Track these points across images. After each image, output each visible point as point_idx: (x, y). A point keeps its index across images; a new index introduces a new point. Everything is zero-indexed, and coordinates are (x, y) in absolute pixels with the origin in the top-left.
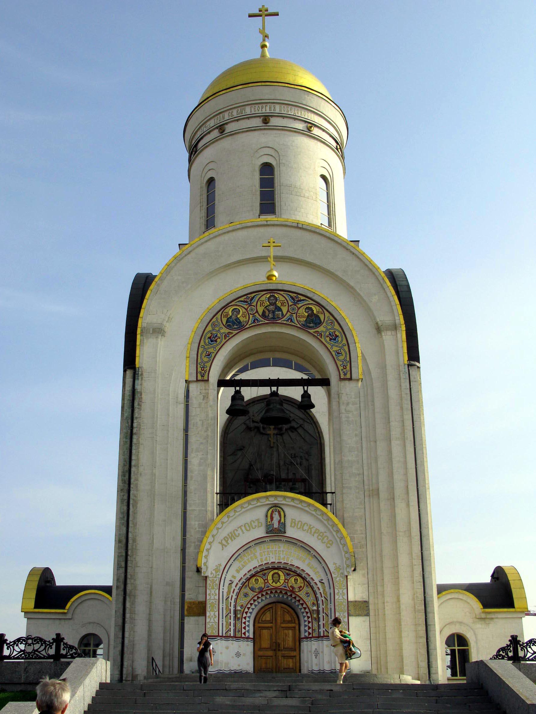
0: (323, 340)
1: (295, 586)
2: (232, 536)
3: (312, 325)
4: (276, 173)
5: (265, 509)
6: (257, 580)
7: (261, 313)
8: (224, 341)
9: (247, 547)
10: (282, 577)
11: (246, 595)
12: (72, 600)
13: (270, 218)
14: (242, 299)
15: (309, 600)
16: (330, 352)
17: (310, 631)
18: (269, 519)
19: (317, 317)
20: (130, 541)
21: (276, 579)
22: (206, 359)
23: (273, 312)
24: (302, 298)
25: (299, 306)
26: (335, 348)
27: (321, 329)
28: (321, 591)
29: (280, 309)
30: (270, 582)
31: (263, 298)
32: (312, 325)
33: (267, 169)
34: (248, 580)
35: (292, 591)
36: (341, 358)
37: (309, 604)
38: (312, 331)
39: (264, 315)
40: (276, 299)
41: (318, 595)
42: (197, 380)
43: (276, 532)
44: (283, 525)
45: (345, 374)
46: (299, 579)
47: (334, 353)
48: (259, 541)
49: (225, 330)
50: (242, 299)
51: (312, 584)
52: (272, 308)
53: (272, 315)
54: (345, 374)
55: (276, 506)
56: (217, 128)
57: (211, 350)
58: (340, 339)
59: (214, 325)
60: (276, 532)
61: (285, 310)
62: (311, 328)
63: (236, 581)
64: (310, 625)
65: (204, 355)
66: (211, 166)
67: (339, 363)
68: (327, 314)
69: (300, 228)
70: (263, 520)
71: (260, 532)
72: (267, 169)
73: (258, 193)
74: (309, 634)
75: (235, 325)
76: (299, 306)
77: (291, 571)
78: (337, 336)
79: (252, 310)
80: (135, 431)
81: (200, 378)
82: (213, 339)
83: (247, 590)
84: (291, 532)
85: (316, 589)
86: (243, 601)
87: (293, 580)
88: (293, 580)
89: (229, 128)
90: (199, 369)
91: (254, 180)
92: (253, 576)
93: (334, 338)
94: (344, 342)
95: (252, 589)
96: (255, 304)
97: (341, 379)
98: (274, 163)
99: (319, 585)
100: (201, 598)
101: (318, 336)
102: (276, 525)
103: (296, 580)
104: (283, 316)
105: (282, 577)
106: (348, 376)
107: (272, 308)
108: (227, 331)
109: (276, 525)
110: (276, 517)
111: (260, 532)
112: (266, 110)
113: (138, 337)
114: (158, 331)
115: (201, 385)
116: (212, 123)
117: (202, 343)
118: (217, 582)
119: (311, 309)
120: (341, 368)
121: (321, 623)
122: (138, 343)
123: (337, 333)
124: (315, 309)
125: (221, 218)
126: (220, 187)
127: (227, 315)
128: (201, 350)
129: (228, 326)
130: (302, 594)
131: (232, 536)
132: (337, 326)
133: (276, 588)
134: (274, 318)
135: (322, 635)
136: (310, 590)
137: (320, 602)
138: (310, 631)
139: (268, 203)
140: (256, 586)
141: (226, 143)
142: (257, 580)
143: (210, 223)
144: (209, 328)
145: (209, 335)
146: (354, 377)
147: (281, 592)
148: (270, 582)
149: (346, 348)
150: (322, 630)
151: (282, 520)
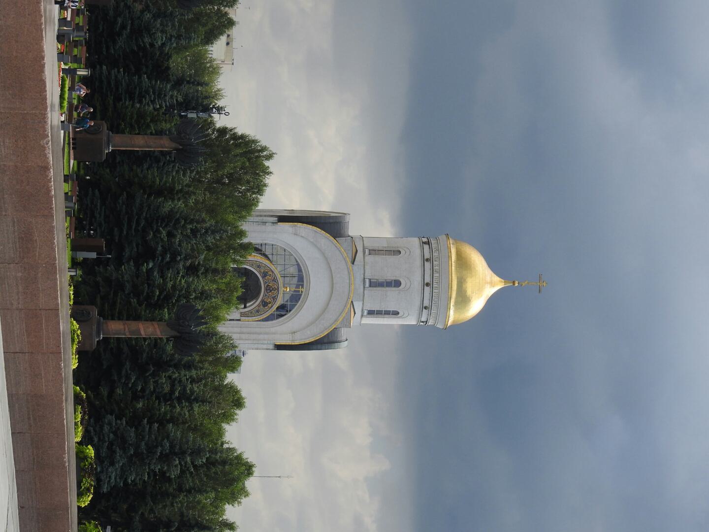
4: (394, 289)
7: (269, 284)
13: (367, 284)
27: (262, 307)
29: (271, 291)
33: (397, 284)
38: (261, 303)
45: (243, 314)
49: (262, 271)
52: (271, 289)
53: (268, 289)
54: (243, 314)
59: (264, 267)
61: (270, 293)
62: (262, 302)
66: (408, 253)
72: (397, 284)
75: (265, 275)
82: (259, 267)
91: (390, 276)
93: (258, 311)
98: (400, 288)
107: (271, 289)
117: (257, 262)
124: (270, 305)
129: (264, 272)
141: (418, 262)
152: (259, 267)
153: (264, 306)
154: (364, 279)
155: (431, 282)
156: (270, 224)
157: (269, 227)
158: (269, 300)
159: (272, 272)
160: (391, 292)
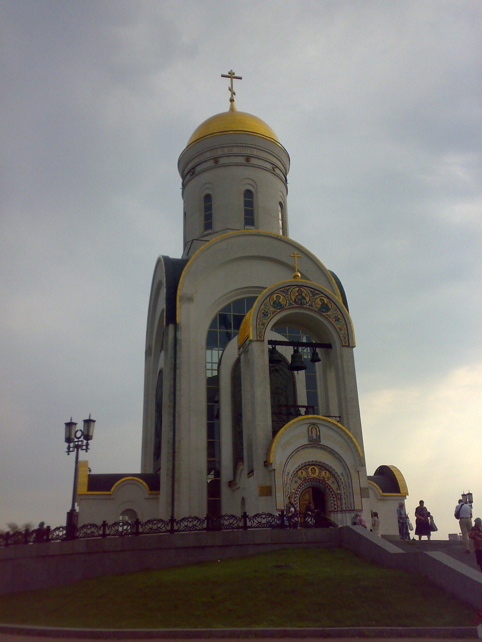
0: (331, 320)
1: (325, 477)
3: (324, 310)
4: (255, 197)
5: (307, 426)
6: (302, 472)
8: (272, 316)
9: (297, 450)
10: (317, 471)
11: (296, 482)
12: (116, 484)
14: (281, 290)
15: (334, 487)
16: (336, 329)
17: (336, 507)
18: (310, 433)
19: (328, 306)
20: (177, 443)
21: (313, 472)
22: (262, 327)
23: (301, 300)
24: (318, 292)
25: (316, 297)
26: (338, 326)
27: (329, 313)
28: (343, 480)
29: (305, 299)
30: (310, 474)
31: (294, 290)
32: (324, 310)
33: (249, 194)
34: (297, 472)
35: (324, 480)
36: (343, 332)
37: (335, 489)
38: (324, 314)
39: (295, 302)
40: (302, 292)
41: (340, 483)
42: (257, 341)
43: (315, 442)
46: (327, 473)
47: (338, 329)
48: (304, 447)
49: (272, 309)
50: (281, 290)
51: (336, 476)
52: (300, 297)
55: (314, 424)
56: (212, 159)
57: (264, 321)
58: (341, 321)
61: (308, 299)
63: (291, 472)
64: (335, 503)
65: (260, 324)
67: (341, 336)
68: (333, 304)
69: (279, 239)
70: (306, 433)
71: (305, 441)
72: (249, 194)
73: (243, 210)
74: (335, 509)
76: (316, 297)
77: (322, 466)
78: (339, 318)
79: (288, 297)
80: (178, 366)
81: (259, 339)
82: (265, 314)
83: (297, 479)
84: (323, 442)
85: (338, 479)
86: (296, 486)
87: (323, 472)
88: (323, 472)
89: (222, 161)
90: (258, 333)
91: (240, 201)
92: (300, 469)
94: (344, 322)
95: (300, 478)
96: (289, 293)
99: (341, 477)
100: (268, 484)
102: (314, 437)
103: (325, 473)
104: (307, 303)
105: (317, 471)
106: (347, 344)
107: (300, 297)
108: (274, 309)
109: (314, 437)
110: (314, 431)
111: (305, 441)
112: (248, 152)
113: (178, 302)
114: (190, 299)
115: (259, 343)
116: (208, 155)
118: (282, 473)
119: (323, 300)
120: (343, 339)
121: (343, 501)
122: (178, 306)
123: (339, 317)
124: (326, 300)
125: (217, 225)
126: (216, 203)
127: (273, 299)
128: (258, 321)
129: (274, 307)
130: (329, 482)
132: (339, 312)
133: (314, 478)
134: (301, 304)
135: (344, 509)
136: (334, 480)
137: (342, 488)
138: (336, 507)
139: (250, 218)
140: (302, 476)
142: (302, 472)
143: (208, 225)
144: (263, 307)
145: (263, 311)
146: (351, 345)
147: (316, 481)
148: (310, 474)
149: (345, 326)
150: (344, 506)
151: (318, 434)
152: (265, 314)
153: (328, 309)
157: (183, 335)
158: (318, 300)
159: (271, 294)
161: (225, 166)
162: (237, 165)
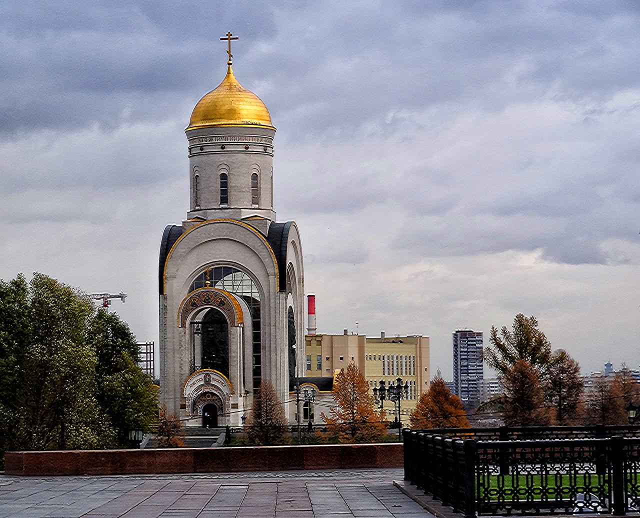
2: (194, 384)
13: (226, 206)
27: (224, 307)
43: (208, 383)
44: (209, 379)
52: (207, 298)
60: (208, 383)
61: (212, 299)
62: (221, 306)
66: (196, 168)
97: (231, 326)
101: (223, 309)
107: (207, 298)
110: (208, 377)
129: (192, 306)
131: (194, 384)
153: (224, 305)
154: (220, 209)
155: (220, 145)
156: (166, 301)
160: (232, 182)
161: (207, 154)
162: (215, 153)
